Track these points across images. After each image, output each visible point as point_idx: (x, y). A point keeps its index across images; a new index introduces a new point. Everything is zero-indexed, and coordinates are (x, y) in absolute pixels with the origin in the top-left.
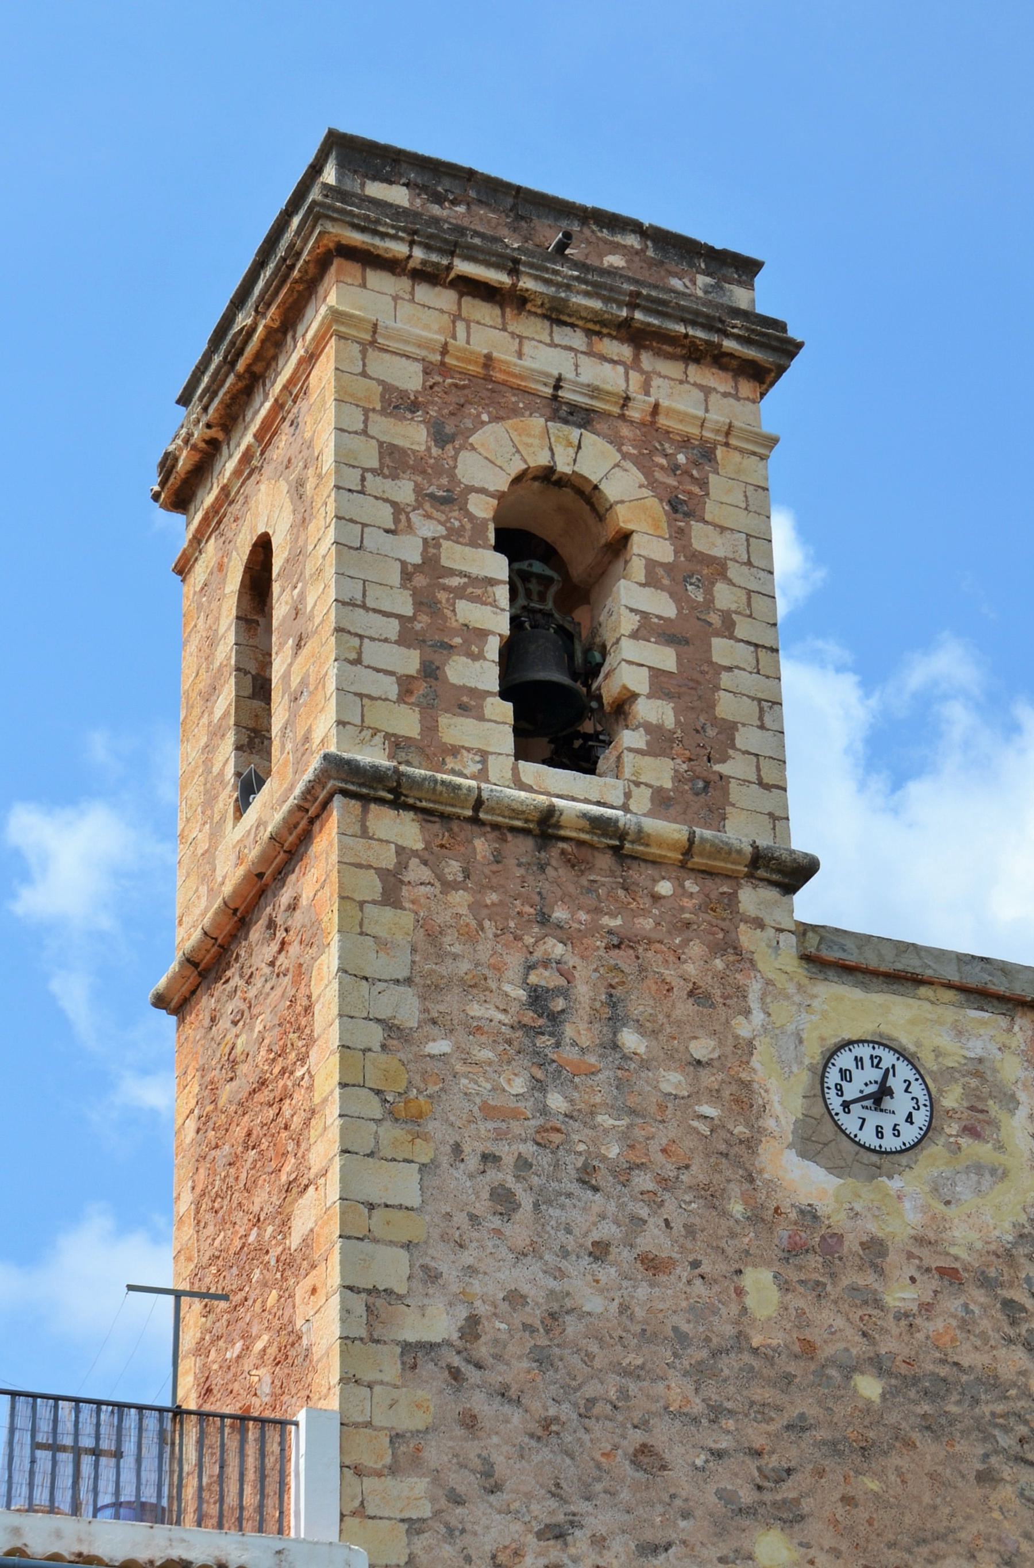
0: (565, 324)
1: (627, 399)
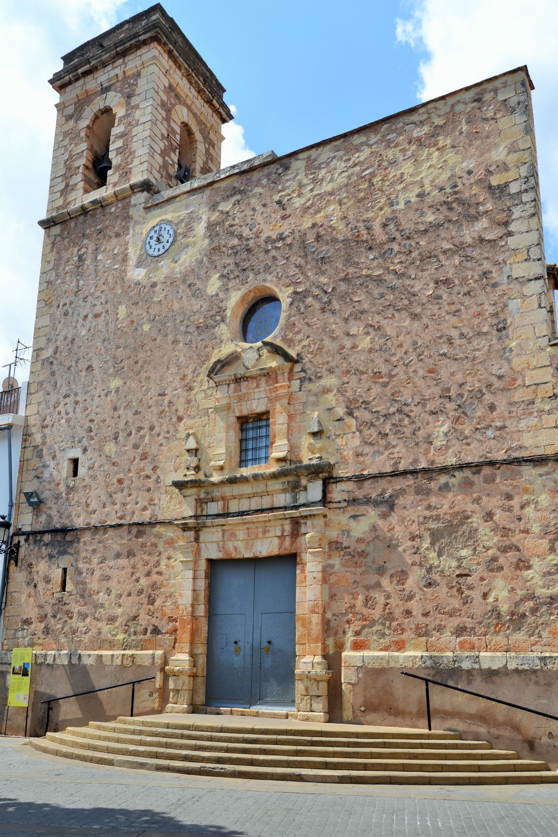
1: (117, 75)
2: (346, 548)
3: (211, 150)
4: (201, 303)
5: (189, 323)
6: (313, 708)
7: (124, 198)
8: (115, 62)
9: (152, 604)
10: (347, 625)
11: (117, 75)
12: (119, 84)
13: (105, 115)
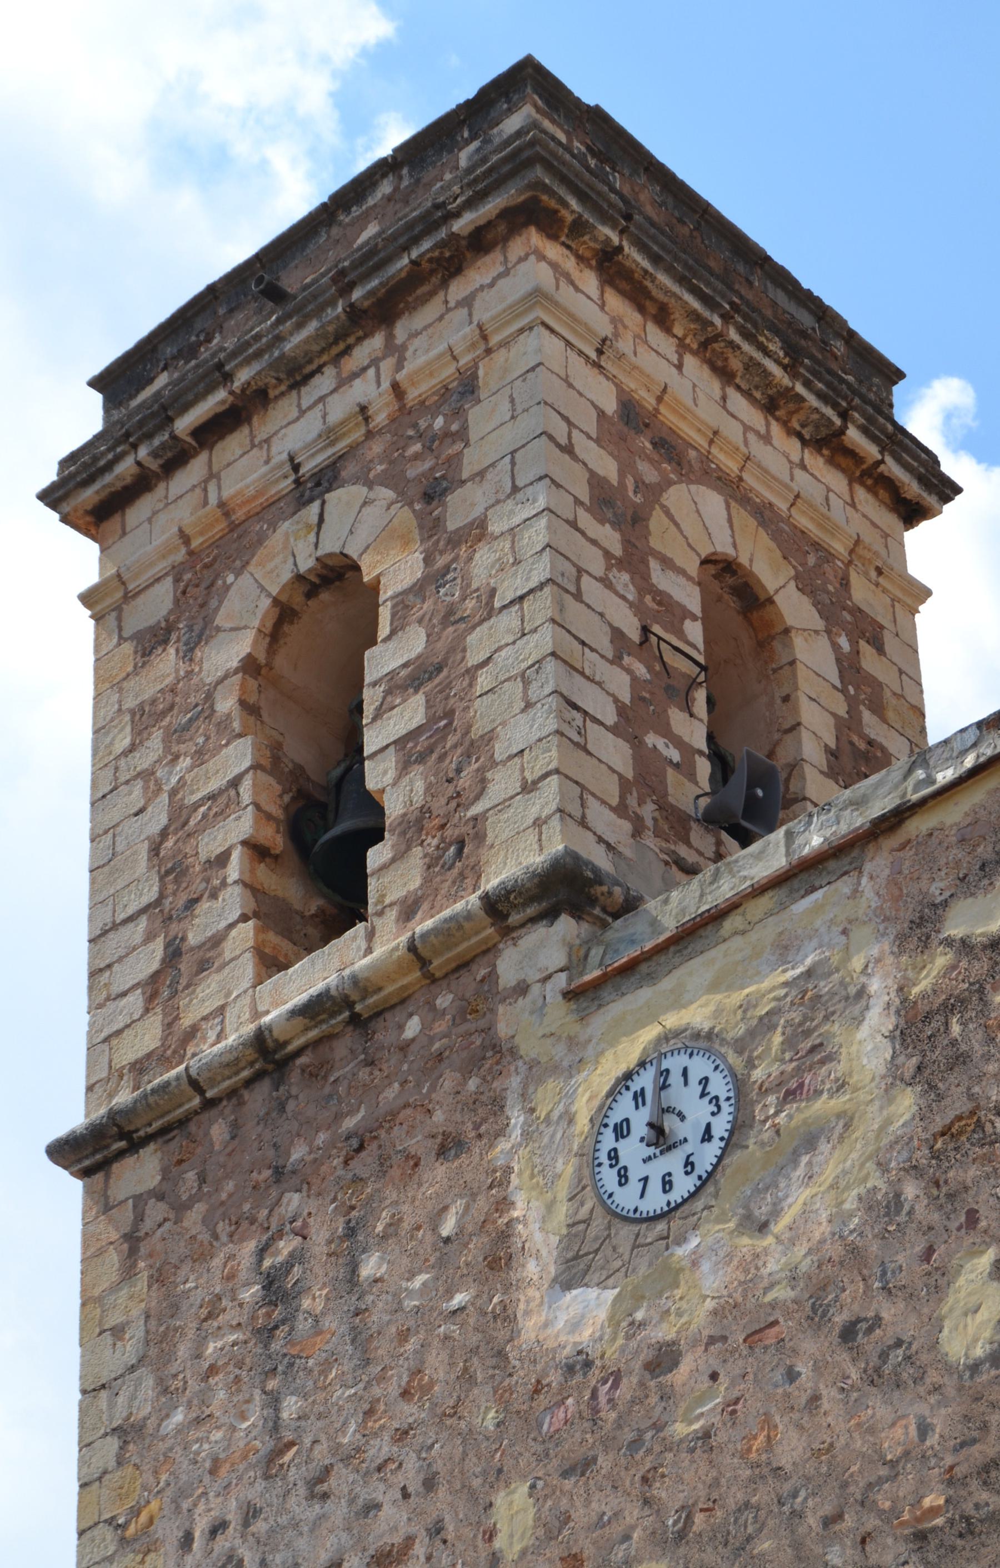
0: (312, 375)
1: (363, 409)
3: (870, 661)
4: (922, 1409)
5: (872, 1522)
7: (464, 965)
8: (347, 351)
11: (363, 409)
12: (377, 447)
13: (325, 596)
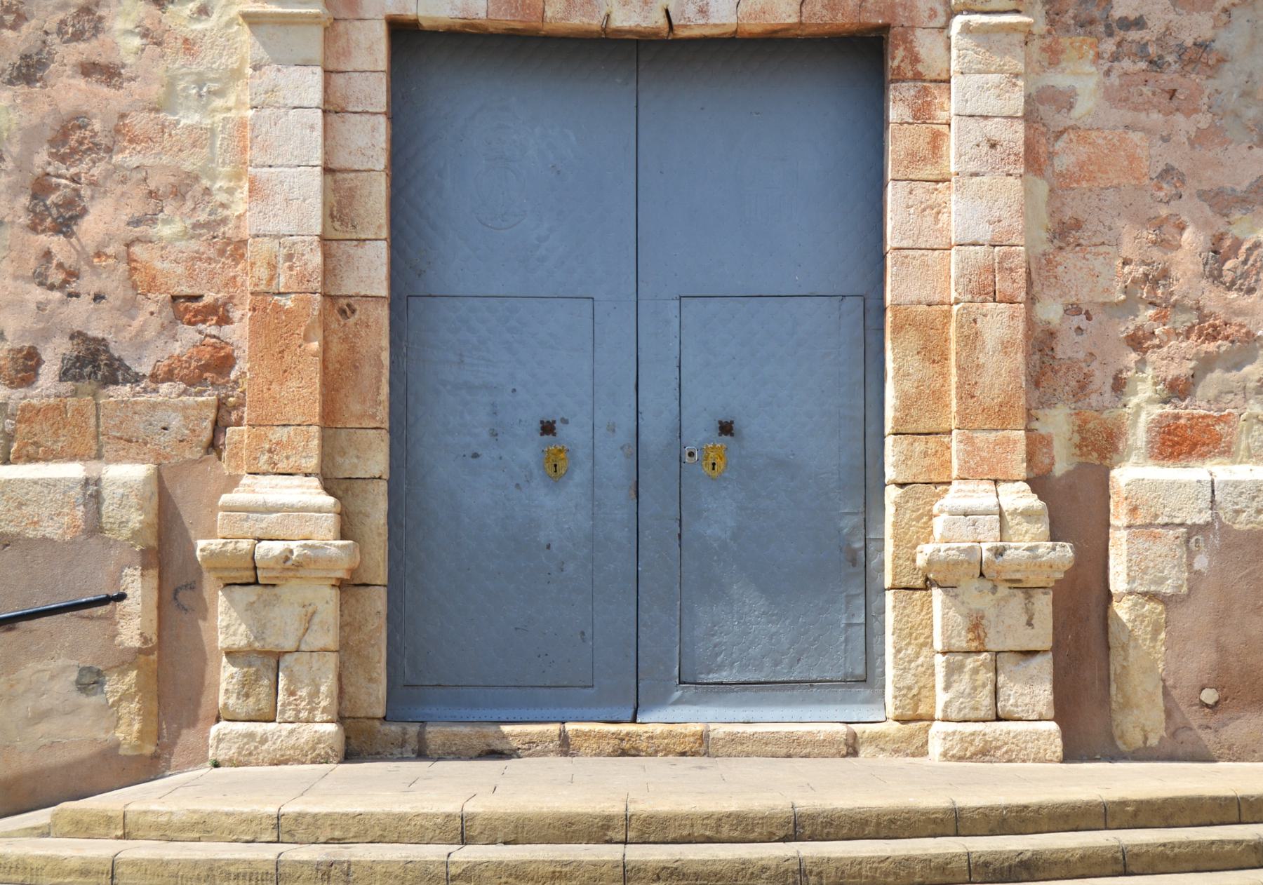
2: (1126, 24)
6: (1006, 705)
9: (65, 225)
10: (1133, 356)
